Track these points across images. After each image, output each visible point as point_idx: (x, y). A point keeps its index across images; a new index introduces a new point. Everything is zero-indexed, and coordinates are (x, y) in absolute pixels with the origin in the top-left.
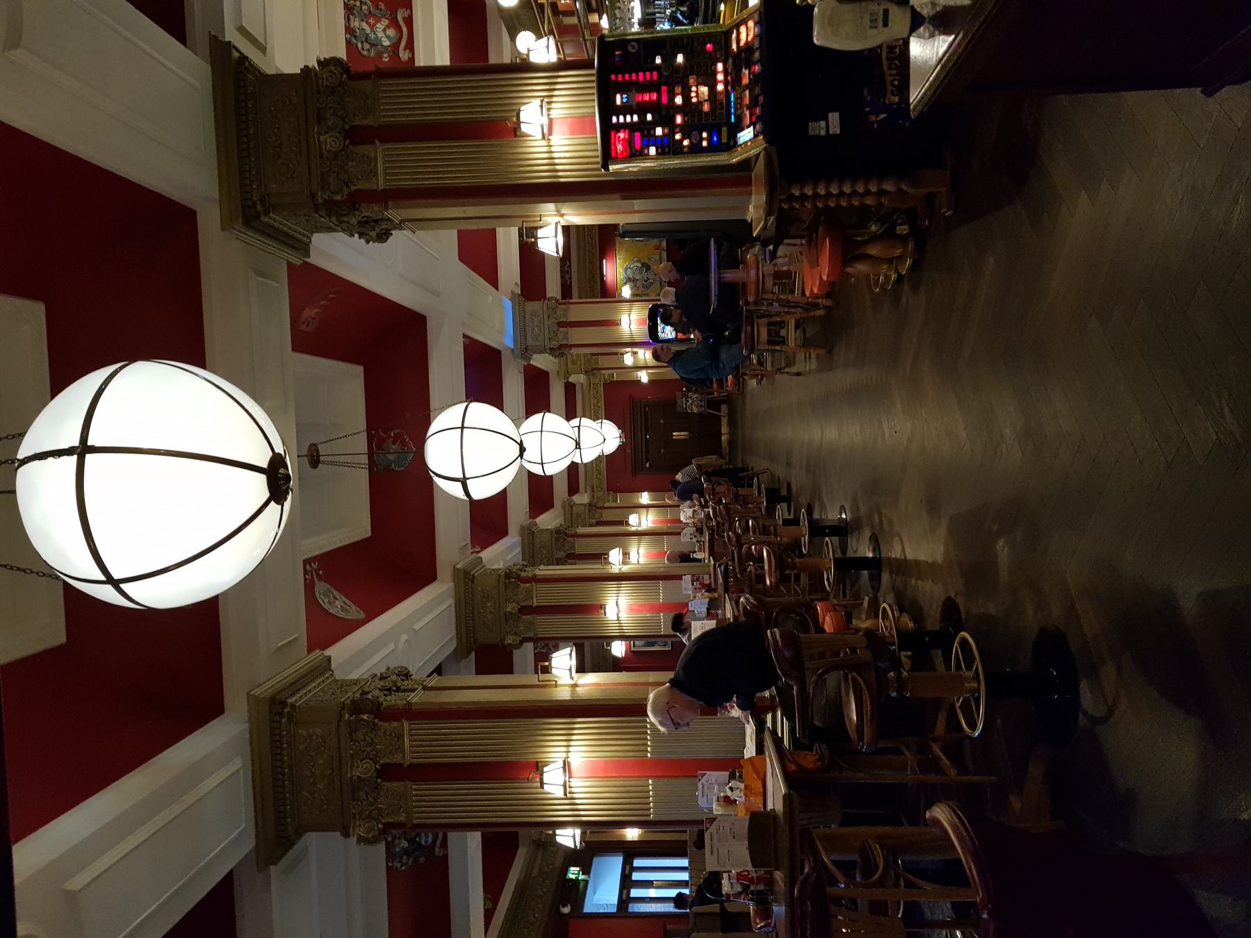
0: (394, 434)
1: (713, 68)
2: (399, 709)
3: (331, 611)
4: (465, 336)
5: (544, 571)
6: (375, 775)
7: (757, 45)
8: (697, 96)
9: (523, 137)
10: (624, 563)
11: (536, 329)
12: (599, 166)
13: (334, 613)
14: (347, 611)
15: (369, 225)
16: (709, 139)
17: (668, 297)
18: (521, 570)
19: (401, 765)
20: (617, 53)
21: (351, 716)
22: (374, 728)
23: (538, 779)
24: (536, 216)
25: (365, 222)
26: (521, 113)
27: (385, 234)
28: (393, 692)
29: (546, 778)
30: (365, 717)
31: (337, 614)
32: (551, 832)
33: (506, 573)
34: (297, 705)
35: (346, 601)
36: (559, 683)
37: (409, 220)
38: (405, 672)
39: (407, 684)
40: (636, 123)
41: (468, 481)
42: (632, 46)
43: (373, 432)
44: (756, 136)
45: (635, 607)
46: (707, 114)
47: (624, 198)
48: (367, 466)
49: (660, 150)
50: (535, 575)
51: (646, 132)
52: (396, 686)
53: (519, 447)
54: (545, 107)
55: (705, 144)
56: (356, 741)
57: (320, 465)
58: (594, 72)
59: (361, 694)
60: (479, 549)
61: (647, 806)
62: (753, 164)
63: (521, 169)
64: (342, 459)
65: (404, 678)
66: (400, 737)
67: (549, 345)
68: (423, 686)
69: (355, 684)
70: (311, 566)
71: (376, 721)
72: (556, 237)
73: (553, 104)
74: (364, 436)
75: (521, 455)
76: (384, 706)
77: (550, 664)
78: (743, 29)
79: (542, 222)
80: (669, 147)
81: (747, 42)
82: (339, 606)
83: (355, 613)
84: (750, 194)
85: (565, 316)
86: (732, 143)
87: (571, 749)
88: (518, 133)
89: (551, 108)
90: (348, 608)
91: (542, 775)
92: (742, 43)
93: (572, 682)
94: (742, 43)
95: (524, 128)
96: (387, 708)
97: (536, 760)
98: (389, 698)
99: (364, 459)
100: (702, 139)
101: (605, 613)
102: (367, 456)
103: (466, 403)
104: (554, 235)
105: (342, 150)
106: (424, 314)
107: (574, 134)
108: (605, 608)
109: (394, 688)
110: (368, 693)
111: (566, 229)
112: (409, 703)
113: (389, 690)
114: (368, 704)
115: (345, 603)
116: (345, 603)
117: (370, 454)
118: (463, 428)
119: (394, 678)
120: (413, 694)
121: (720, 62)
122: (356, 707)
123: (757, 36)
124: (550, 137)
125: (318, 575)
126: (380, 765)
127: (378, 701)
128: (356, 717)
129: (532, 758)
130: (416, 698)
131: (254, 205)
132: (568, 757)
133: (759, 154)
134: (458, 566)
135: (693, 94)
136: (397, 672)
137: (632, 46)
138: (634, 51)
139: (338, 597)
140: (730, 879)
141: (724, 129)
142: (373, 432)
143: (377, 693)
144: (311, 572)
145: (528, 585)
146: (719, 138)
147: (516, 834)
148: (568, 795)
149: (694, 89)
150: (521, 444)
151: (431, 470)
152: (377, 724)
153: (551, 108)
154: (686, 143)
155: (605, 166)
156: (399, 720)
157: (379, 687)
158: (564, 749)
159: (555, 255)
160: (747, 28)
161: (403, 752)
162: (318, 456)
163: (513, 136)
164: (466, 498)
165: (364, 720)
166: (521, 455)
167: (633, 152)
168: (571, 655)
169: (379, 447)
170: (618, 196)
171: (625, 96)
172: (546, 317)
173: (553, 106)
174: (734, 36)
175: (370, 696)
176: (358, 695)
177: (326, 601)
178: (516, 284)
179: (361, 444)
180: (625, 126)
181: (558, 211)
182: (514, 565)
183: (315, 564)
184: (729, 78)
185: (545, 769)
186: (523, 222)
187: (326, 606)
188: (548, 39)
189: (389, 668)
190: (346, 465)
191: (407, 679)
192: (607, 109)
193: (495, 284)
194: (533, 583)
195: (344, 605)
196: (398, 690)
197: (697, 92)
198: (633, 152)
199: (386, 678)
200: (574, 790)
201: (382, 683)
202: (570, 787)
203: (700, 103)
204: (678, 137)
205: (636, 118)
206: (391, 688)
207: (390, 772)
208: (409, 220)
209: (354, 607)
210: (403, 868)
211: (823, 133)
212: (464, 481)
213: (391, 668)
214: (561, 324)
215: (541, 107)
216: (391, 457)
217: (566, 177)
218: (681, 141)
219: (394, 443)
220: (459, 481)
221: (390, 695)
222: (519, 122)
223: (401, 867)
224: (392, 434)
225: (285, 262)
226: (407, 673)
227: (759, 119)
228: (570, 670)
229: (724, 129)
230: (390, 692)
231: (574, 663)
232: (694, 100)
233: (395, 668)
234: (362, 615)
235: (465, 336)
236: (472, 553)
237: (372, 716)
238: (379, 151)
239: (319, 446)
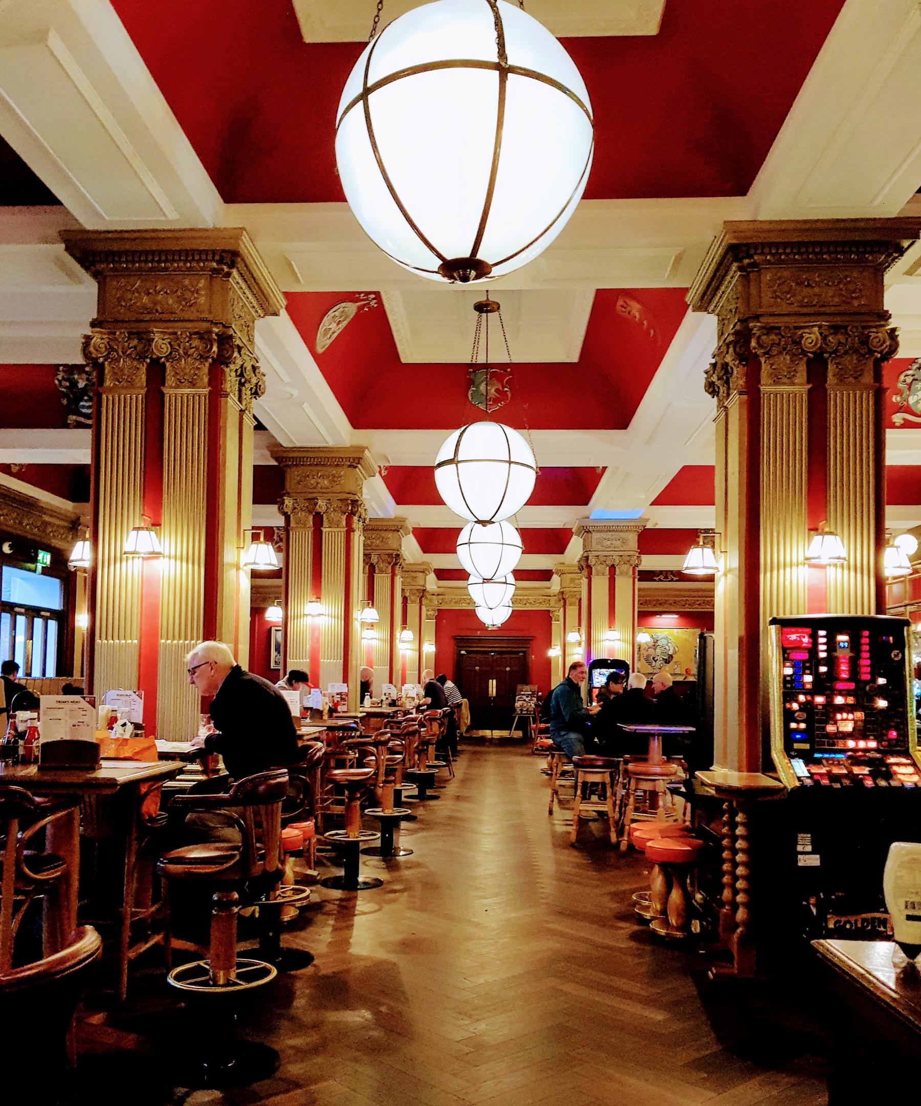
1: (872, 737)
2: (222, 384)
3: (325, 318)
4: (605, 468)
5: (358, 539)
6: (154, 356)
7: (894, 783)
8: (843, 720)
9: (809, 538)
12: (775, 615)
13: (323, 322)
14: (325, 335)
16: (797, 731)
17: (636, 681)
19: (164, 384)
20: (891, 638)
21: (217, 334)
22: (203, 358)
23: (142, 525)
24: (726, 547)
26: (833, 536)
28: (239, 378)
29: (143, 534)
30: (215, 349)
32: (87, 536)
35: (335, 335)
36: (242, 551)
37: (727, 415)
38: (259, 392)
39: (246, 393)
40: (817, 654)
42: (898, 654)
43: (509, 370)
44: (799, 779)
46: (824, 729)
47: (740, 640)
48: (474, 362)
49: (788, 678)
50: (354, 531)
51: (808, 665)
52: (245, 382)
54: (839, 562)
55: (793, 725)
56: (190, 339)
57: (478, 313)
58: (873, 614)
59: (238, 346)
61: (110, 637)
62: (770, 774)
63: (775, 534)
65: (253, 391)
66: (193, 384)
67: (591, 555)
68: (244, 411)
69: (249, 340)
70: (374, 299)
71: (210, 360)
72: (704, 567)
74: (505, 359)
75: (479, 522)
76: (225, 369)
77: (261, 543)
78: (911, 770)
80: (792, 688)
81: (896, 773)
83: (323, 342)
84: (740, 770)
85: (621, 573)
86: (793, 753)
88: (812, 532)
89: (836, 567)
90: (329, 336)
92: (895, 768)
93: (242, 565)
94: (895, 768)
95: (817, 539)
96: (223, 373)
97: (163, 524)
98: (233, 374)
99: (481, 360)
100: (798, 722)
104: (705, 565)
106: (629, 428)
107: (809, 590)
109: (243, 380)
110: (239, 352)
111: (711, 579)
112: (227, 395)
113: (242, 375)
115: (333, 333)
116: (333, 333)
117: (486, 366)
119: (254, 381)
120: (236, 399)
121: (878, 744)
122: (225, 340)
123: (902, 784)
125: (364, 306)
126: (164, 362)
127: (230, 363)
128: (215, 340)
129: (165, 519)
130: (231, 405)
133: (780, 781)
134: (366, 452)
135: (845, 715)
136: (259, 384)
137: (898, 654)
138: (893, 656)
139: (340, 326)
140: (31, 719)
141: (807, 746)
142: (509, 370)
143: (239, 362)
144: (367, 299)
146: (799, 741)
147: (87, 501)
148: (125, 556)
149: (851, 716)
150: (490, 522)
152: (206, 361)
153: (836, 567)
154: (795, 706)
155: (774, 621)
156: (210, 384)
157: (245, 365)
158: (173, 553)
159: (685, 566)
160: (911, 774)
161: (177, 387)
162: (487, 312)
163: (810, 527)
164: (437, 462)
165: (211, 348)
166: (479, 522)
167: (788, 651)
168: (270, 564)
169: (494, 375)
170: (743, 633)
171: (846, 644)
172: (621, 553)
173: (839, 570)
174: (904, 760)
175: (236, 354)
176: (238, 342)
177: (337, 313)
179: (498, 356)
180: (815, 644)
181: (730, 570)
184: (860, 753)
185: (153, 533)
187: (331, 314)
188: (908, 568)
190: (476, 341)
191: (252, 394)
192: (834, 625)
193: (657, 502)
194: (346, 529)
196: (241, 384)
197: (847, 719)
198: (788, 651)
199: (254, 372)
200: (130, 562)
201: (249, 368)
202: (133, 558)
203: (835, 722)
204: (802, 698)
205: (823, 655)
206: (244, 377)
207: (157, 372)
208: (727, 415)
209: (329, 342)
210: (57, 382)
211: (800, 848)
213: (264, 378)
216: (482, 387)
218: (797, 701)
219: (497, 391)
221: (237, 376)
222: (824, 533)
223: (58, 380)
224: (506, 389)
226: (258, 394)
227: (817, 782)
228: (254, 563)
229: (807, 746)
230: (239, 376)
231: (262, 567)
232: (839, 716)
233: (264, 382)
234: (320, 350)
235: (605, 468)
236: (380, 467)
237: (215, 356)
239: (497, 313)
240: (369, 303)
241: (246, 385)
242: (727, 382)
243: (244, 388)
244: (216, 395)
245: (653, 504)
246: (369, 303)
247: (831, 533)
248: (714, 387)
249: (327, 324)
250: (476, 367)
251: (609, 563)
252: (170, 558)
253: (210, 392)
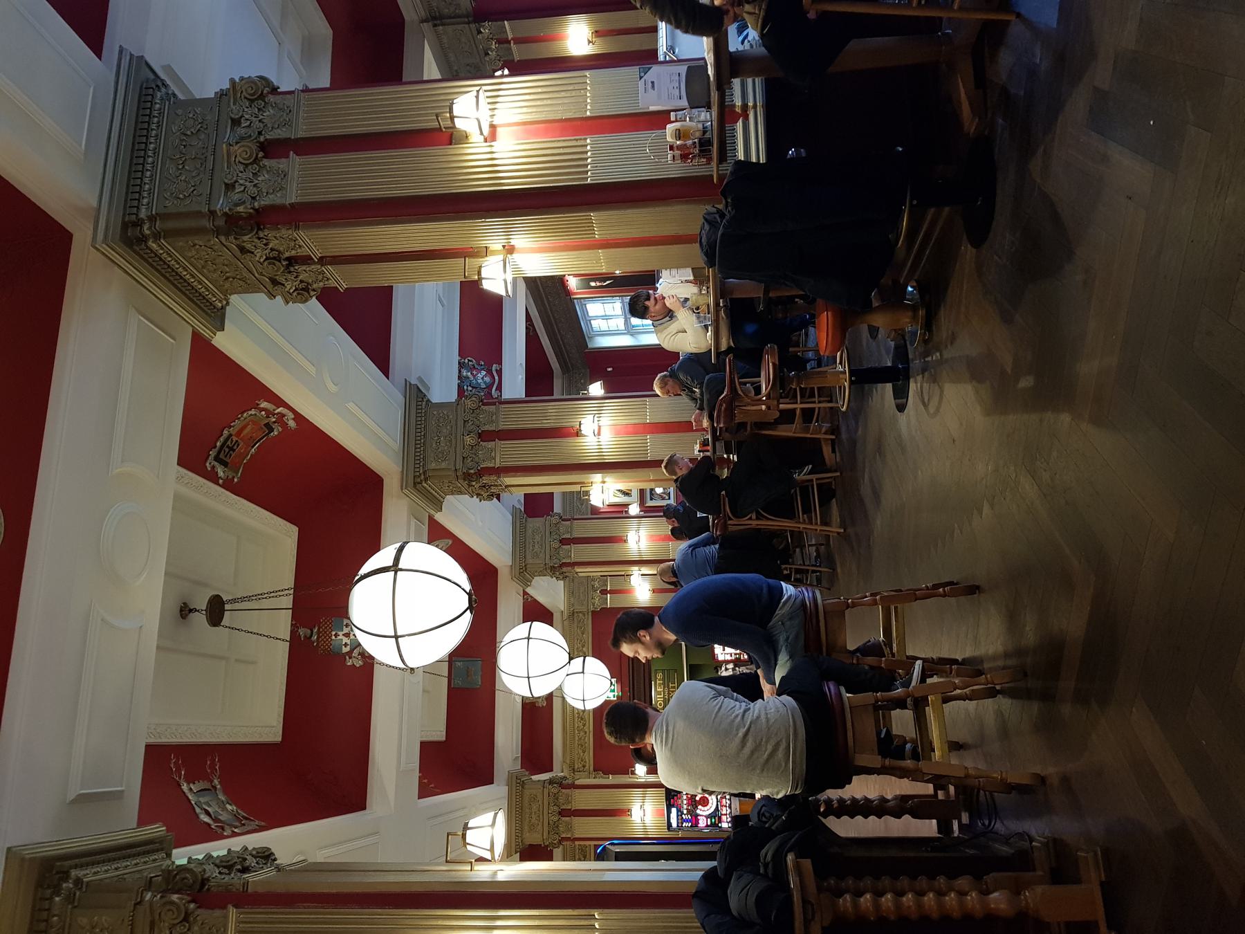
15: (280, 261)
25: (274, 258)
26: (454, 106)
34: (84, 880)
38: (266, 853)
71: (192, 906)
73: (496, 111)
89: (494, 115)
95: (459, 124)
105: (251, 164)
109: (239, 867)
114: (186, 878)
124: (493, 144)
131: (138, 223)
136: (254, 853)
153: (494, 115)
178: (519, 501)
189: (247, 848)
213: (250, 849)
214: (564, 542)
215: (477, 97)
222: (452, 118)
225: (191, 329)
233: (254, 849)
238: (294, 164)
244: (245, 899)
247: (451, 111)
248: (303, 289)
253: (236, 906)
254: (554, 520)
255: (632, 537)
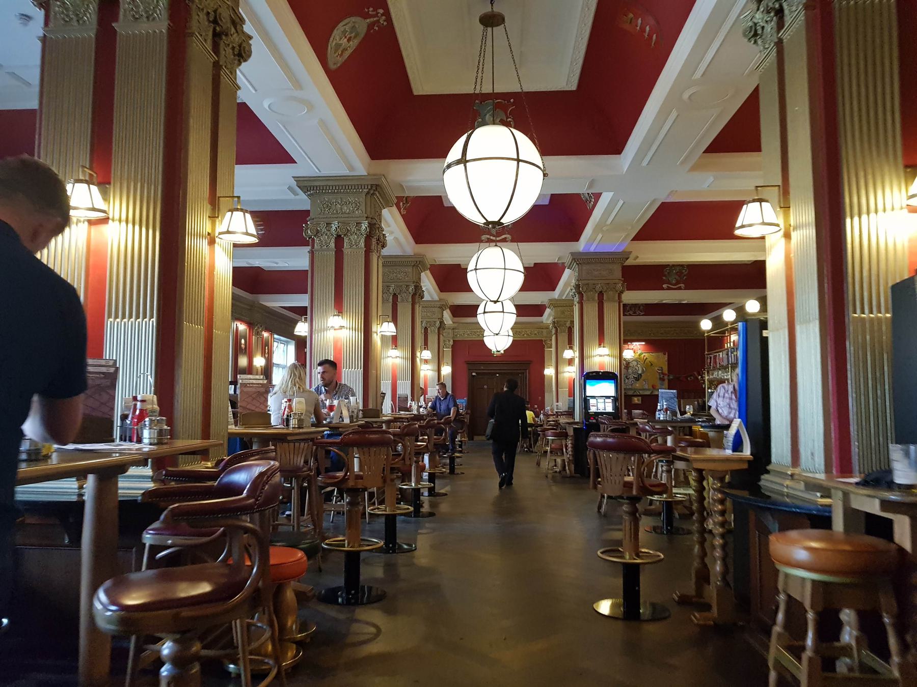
0: (510, 121)
3: (335, 31)
4: (598, 196)
10: (383, 338)
11: (596, 273)
13: (333, 34)
18: (378, 240)
27: (756, 34)
31: (332, 37)
33: (375, 224)
39: (227, 53)
41: (462, 165)
43: (512, 100)
45: (339, 344)
53: (497, 220)
60: (402, 213)
64: (488, 66)
70: (382, 15)
72: (764, 223)
76: (190, 4)
79: (779, 209)
82: (341, 42)
83: (336, 60)
87: (124, 224)
91: (88, 183)
99: (487, 89)
101: (334, 315)
102: (492, 92)
103: (542, 167)
108: (338, 316)
113: (215, 22)
118: (518, 160)
132: (113, 220)
142: (512, 100)
144: (376, 15)
145: (363, 244)
151: (472, 133)
156: (172, 17)
157: (220, 10)
158: (124, 217)
172: (607, 282)
177: (347, 28)
178: (638, 257)
182: (384, 235)
183: (385, 21)
186: (779, 186)
187: (340, 27)
195: (341, 49)
196: (217, 36)
206: (218, 24)
209: (340, 60)
212: (463, 161)
214: (601, 294)
217: (853, 228)
220: (462, 156)
226: (243, 57)
234: (332, 67)
240: (378, 21)
241: (224, 37)
242: (780, 12)
243: (222, 44)
245: (635, 239)
246: (378, 21)
249: (338, 38)
250: (484, 97)
251: (598, 288)
252: (120, 221)
254: (619, 286)
255: (604, 350)
